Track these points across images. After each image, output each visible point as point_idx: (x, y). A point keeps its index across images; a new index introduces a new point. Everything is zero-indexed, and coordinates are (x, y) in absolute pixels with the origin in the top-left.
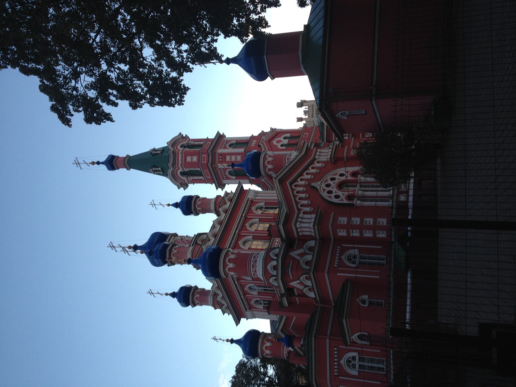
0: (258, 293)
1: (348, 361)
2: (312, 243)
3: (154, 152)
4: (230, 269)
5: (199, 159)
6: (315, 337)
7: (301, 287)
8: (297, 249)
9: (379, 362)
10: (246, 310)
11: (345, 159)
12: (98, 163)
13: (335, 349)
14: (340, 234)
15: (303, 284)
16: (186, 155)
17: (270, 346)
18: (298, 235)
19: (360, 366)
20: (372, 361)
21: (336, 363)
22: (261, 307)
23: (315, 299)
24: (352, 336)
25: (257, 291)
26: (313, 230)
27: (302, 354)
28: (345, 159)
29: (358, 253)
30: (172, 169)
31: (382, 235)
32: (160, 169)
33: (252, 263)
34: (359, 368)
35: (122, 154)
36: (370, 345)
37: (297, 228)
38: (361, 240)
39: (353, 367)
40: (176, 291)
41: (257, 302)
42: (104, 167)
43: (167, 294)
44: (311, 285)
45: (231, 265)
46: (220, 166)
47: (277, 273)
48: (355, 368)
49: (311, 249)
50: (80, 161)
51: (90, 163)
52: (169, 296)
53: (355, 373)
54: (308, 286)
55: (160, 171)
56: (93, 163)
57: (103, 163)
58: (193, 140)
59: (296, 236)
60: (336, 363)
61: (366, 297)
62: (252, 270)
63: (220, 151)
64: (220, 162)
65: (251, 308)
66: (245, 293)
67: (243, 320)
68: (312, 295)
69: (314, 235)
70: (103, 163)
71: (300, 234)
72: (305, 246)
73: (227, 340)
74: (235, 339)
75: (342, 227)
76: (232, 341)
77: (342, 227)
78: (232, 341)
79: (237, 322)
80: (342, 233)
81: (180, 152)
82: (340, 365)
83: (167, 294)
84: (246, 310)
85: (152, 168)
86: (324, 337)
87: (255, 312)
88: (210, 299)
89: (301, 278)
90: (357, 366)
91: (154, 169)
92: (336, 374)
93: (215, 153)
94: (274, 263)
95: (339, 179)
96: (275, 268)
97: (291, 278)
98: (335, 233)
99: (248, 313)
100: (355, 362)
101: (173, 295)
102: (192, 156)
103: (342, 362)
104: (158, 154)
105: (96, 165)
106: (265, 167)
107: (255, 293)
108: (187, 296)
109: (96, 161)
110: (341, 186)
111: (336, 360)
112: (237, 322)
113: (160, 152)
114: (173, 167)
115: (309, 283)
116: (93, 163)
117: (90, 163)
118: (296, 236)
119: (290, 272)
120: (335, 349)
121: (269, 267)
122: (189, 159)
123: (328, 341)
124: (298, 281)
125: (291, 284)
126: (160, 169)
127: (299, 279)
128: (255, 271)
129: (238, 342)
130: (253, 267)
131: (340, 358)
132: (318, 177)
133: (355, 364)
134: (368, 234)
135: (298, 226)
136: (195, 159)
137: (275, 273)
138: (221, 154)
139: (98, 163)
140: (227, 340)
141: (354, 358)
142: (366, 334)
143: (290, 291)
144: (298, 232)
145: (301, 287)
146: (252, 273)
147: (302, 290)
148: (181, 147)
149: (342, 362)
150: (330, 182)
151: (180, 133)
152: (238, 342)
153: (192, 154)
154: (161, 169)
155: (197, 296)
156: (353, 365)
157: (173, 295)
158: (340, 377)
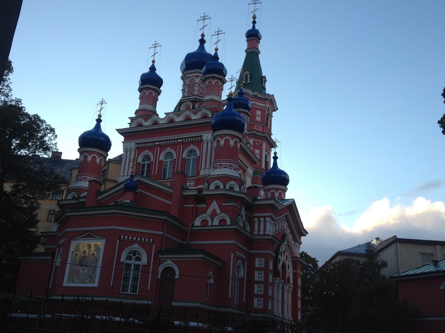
0: (162, 161)
1: (134, 253)
2: (248, 229)
3: (263, 79)
4: (227, 141)
5: (258, 122)
6: (165, 220)
7: (210, 211)
8: (246, 214)
9: (134, 288)
10: (136, 144)
11: (295, 271)
12: (254, 22)
13: (151, 240)
14: (257, 260)
15: (213, 216)
16: (263, 111)
17: (96, 162)
18: (254, 217)
19: (129, 265)
20: (135, 279)
21: (135, 238)
22: (140, 160)
23: (193, 225)
24: (172, 261)
25: (163, 160)
26: (262, 233)
27: (99, 198)
28: (295, 271)
29: (241, 277)
30: (251, 94)
31: (257, 303)
32: (249, 82)
33: (234, 165)
34: (126, 264)
35: (261, 46)
36: (157, 279)
37: (265, 217)
38: (251, 281)
39: (127, 257)
40: (157, 72)
41: (147, 158)
42: (250, 27)
43: (154, 62)
44: (214, 224)
45: (232, 143)
46: (251, 141)
47: (227, 190)
48: (127, 259)
49: (244, 228)
50: (258, 6)
51: (254, 14)
52: (152, 64)
53: (123, 259)
54: (212, 220)
55: (246, 80)
56: (254, 17)
57: (254, 27)
58: (271, 119)
59: (255, 215)
60: (135, 238)
61: (212, 281)
62: (228, 164)
63: (264, 144)
64: (254, 142)
65: (139, 149)
66: (163, 147)
67: (122, 138)
68: (197, 222)
69: (256, 233)
70: (254, 27)
71: (256, 220)
72: (247, 222)
73: (100, 116)
74: (102, 124)
75: (267, 264)
76: (99, 121)
77: (267, 264)
78: (99, 121)
79: (121, 132)
80: (258, 263)
81: (265, 105)
82: (132, 243)
83: (154, 62)
84: (136, 144)
85: (250, 74)
86: (165, 229)
87: (133, 153)
88: (149, 107)
89: (223, 214)
90: (129, 262)
91: (249, 76)
92: (122, 237)
93: (263, 140)
94: (237, 189)
95: (287, 263)
96: (231, 188)
97: (223, 204)
98: (260, 255)
99: (132, 145)
100: (134, 259)
101: (153, 69)
102: (262, 116)
103: (136, 246)
104: (262, 84)
105: (252, 20)
106: (277, 190)
107: (162, 158)
108: (151, 83)
109: (256, 20)
110: (284, 265)
111: (139, 239)
112: (121, 132)
113: (263, 85)
114: (253, 96)
115: (216, 222)
116: (254, 17)
117: (254, 14)
118: (255, 215)
119: (232, 204)
120: (151, 240)
121: (217, 181)
122: (259, 113)
123: (161, 233)
124: (218, 211)
125: (214, 202)
126: (249, 82)
127: (222, 212)
128: (226, 167)
129: (98, 127)
130: (231, 166)
131: (140, 244)
132: (288, 242)
133: (130, 260)
134: (257, 289)
135: (267, 219)
136: (258, 119)
137: (227, 187)
138: (261, 145)
139: (254, 22)
140: (100, 116)
141: (138, 259)
142: (177, 277)
143: (201, 199)
144: (259, 217)
145: (210, 211)
146: (224, 163)
147: (206, 213)
148: (268, 107)
149: (136, 246)
150: (286, 254)
151: (277, 109)
152: (98, 127)
153: (262, 116)
154: (249, 83)
155: (154, 95)
156: (131, 257)
157: (153, 69)
158: (118, 241)
